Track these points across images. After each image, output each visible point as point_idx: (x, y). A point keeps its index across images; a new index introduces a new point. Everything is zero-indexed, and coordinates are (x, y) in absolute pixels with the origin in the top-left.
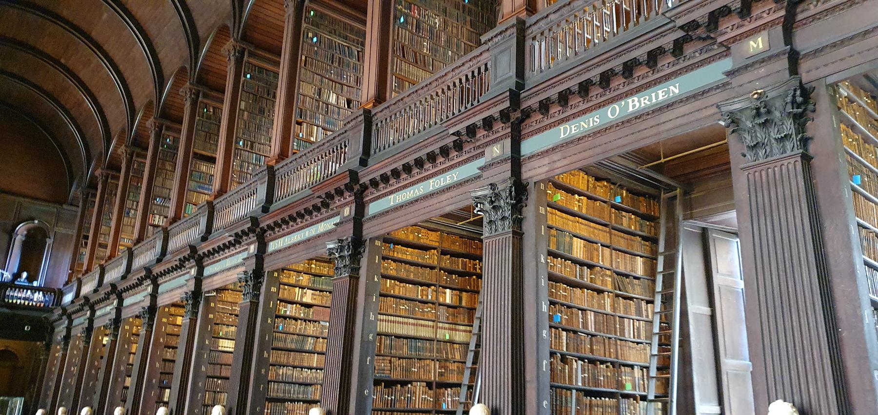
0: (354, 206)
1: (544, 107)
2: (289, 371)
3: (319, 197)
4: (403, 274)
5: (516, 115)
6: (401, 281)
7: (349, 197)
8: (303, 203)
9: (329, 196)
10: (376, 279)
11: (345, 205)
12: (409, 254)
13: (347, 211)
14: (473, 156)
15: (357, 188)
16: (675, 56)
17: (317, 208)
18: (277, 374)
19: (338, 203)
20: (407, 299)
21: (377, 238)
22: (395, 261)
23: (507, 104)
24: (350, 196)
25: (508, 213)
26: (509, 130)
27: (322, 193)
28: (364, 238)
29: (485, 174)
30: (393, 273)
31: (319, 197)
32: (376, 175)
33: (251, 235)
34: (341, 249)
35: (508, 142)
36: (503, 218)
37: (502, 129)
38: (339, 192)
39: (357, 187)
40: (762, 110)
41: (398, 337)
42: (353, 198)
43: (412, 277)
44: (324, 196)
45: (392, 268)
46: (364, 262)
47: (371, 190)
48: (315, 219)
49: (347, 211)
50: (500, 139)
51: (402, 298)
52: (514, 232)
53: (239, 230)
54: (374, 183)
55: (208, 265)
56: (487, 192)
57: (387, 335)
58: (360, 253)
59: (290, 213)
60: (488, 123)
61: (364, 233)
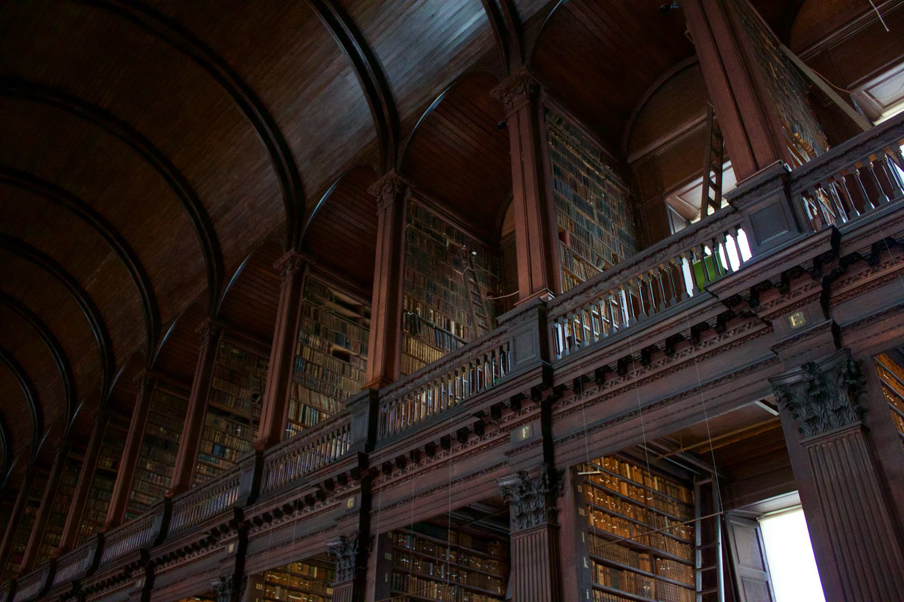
0: (359, 496)
1: (579, 385)
3: (318, 485)
5: (547, 394)
9: (330, 484)
13: (350, 503)
15: (365, 474)
16: (667, 355)
19: (340, 493)
23: (539, 381)
25: (542, 505)
26: (539, 410)
28: (372, 533)
34: (345, 547)
35: (538, 424)
36: (537, 511)
37: (532, 409)
38: (343, 480)
40: (817, 382)
44: (323, 485)
47: (383, 477)
49: (350, 503)
52: (549, 526)
60: (517, 402)
61: (372, 526)
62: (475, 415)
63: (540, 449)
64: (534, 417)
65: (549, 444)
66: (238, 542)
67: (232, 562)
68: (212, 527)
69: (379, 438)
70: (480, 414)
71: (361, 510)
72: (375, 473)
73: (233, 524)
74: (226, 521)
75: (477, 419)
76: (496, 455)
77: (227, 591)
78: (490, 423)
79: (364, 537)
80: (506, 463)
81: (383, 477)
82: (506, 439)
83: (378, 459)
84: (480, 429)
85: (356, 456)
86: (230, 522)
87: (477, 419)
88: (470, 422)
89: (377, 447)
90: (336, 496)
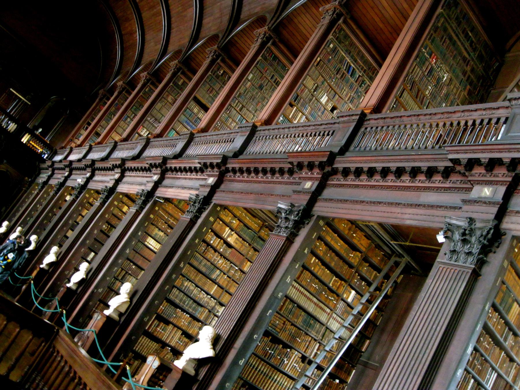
2: (192, 287)
3: (291, 163)
4: (327, 259)
6: (324, 264)
7: (317, 173)
8: (272, 163)
9: (300, 166)
10: (306, 251)
11: (310, 179)
12: (339, 245)
13: (308, 185)
14: (456, 188)
17: (282, 172)
18: (182, 284)
19: (304, 174)
20: (321, 281)
21: (323, 218)
22: (327, 244)
24: (318, 174)
26: (510, 179)
27: (295, 161)
29: (465, 208)
30: (321, 254)
31: (291, 163)
32: (353, 166)
33: (216, 169)
34: (290, 212)
35: (502, 190)
38: (311, 166)
39: (328, 169)
41: (300, 307)
42: (320, 176)
43: (332, 265)
44: (295, 164)
45: (321, 249)
46: (303, 233)
48: (275, 179)
49: (308, 185)
50: (497, 183)
51: (317, 277)
53: (208, 162)
54: (346, 172)
55: (169, 178)
56: (463, 224)
57: (292, 301)
58: (303, 224)
59: (257, 165)
60: (493, 164)
62: (451, 160)
63: (494, 210)
64: (502, 183)
65: (502, 211)
66: (216, 179)
67: (208, 190)
68: (205, 161)
69: (352, 148)
70: (456, 162)
71: (313, 193)
72: (335, 172)
73: (218, 165)
74: (215, 161)
75: (450, 164)
76: (455, 198)
77: (197, 204)
78: (459, 172)
79: (307, 213)
80: (460, 208)
81: (339, 176)
82: (470, 190)
83: (340, 164)
84: (447, 173)
85: (329, 153)
86: (217, 163)
87: (450, 164)
88: (442, 165)
89: (348, 154)
90: (301, 176)
